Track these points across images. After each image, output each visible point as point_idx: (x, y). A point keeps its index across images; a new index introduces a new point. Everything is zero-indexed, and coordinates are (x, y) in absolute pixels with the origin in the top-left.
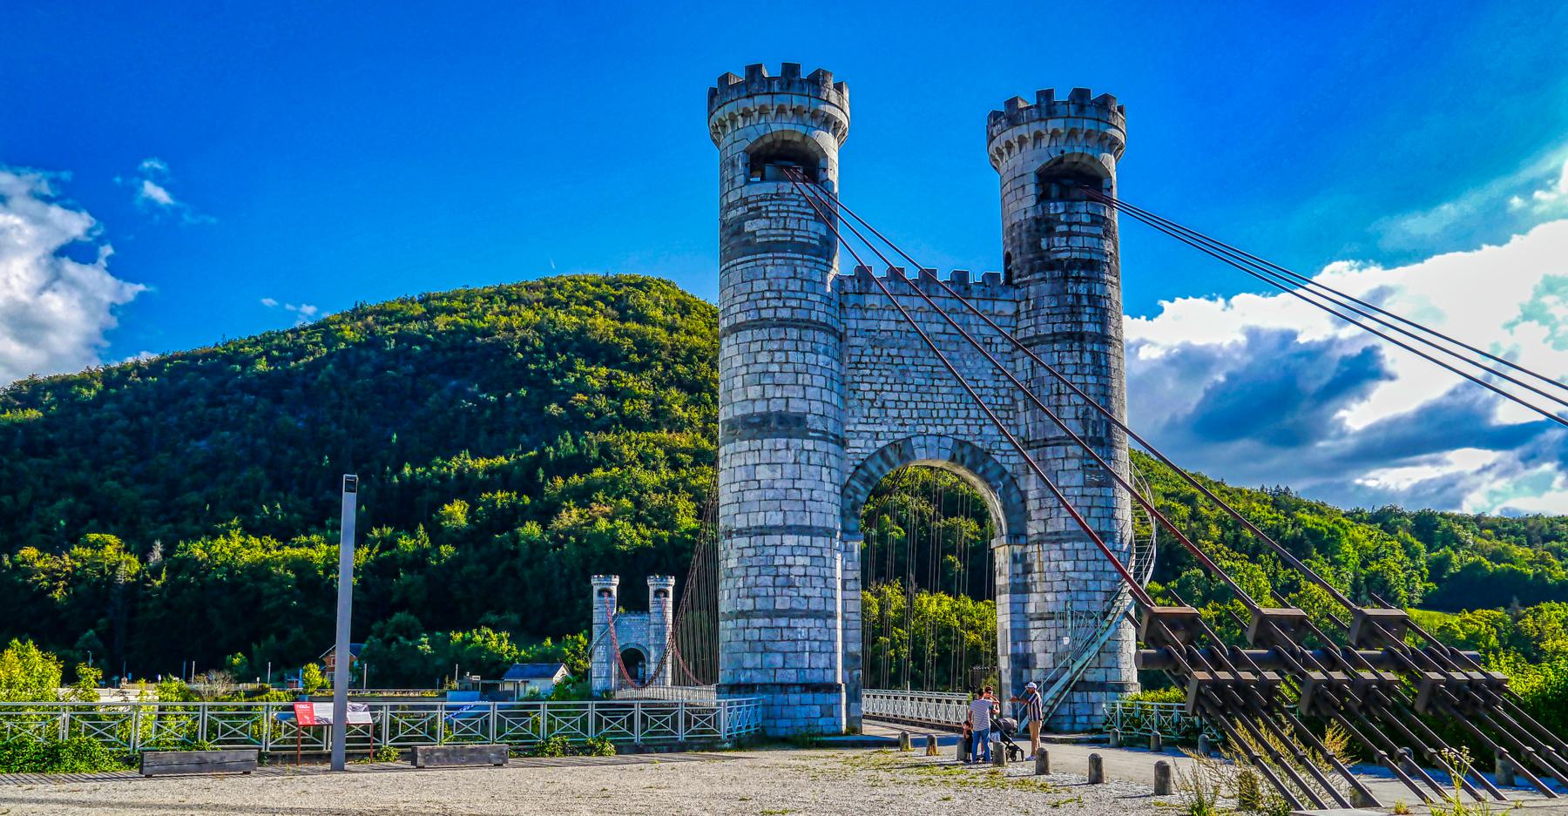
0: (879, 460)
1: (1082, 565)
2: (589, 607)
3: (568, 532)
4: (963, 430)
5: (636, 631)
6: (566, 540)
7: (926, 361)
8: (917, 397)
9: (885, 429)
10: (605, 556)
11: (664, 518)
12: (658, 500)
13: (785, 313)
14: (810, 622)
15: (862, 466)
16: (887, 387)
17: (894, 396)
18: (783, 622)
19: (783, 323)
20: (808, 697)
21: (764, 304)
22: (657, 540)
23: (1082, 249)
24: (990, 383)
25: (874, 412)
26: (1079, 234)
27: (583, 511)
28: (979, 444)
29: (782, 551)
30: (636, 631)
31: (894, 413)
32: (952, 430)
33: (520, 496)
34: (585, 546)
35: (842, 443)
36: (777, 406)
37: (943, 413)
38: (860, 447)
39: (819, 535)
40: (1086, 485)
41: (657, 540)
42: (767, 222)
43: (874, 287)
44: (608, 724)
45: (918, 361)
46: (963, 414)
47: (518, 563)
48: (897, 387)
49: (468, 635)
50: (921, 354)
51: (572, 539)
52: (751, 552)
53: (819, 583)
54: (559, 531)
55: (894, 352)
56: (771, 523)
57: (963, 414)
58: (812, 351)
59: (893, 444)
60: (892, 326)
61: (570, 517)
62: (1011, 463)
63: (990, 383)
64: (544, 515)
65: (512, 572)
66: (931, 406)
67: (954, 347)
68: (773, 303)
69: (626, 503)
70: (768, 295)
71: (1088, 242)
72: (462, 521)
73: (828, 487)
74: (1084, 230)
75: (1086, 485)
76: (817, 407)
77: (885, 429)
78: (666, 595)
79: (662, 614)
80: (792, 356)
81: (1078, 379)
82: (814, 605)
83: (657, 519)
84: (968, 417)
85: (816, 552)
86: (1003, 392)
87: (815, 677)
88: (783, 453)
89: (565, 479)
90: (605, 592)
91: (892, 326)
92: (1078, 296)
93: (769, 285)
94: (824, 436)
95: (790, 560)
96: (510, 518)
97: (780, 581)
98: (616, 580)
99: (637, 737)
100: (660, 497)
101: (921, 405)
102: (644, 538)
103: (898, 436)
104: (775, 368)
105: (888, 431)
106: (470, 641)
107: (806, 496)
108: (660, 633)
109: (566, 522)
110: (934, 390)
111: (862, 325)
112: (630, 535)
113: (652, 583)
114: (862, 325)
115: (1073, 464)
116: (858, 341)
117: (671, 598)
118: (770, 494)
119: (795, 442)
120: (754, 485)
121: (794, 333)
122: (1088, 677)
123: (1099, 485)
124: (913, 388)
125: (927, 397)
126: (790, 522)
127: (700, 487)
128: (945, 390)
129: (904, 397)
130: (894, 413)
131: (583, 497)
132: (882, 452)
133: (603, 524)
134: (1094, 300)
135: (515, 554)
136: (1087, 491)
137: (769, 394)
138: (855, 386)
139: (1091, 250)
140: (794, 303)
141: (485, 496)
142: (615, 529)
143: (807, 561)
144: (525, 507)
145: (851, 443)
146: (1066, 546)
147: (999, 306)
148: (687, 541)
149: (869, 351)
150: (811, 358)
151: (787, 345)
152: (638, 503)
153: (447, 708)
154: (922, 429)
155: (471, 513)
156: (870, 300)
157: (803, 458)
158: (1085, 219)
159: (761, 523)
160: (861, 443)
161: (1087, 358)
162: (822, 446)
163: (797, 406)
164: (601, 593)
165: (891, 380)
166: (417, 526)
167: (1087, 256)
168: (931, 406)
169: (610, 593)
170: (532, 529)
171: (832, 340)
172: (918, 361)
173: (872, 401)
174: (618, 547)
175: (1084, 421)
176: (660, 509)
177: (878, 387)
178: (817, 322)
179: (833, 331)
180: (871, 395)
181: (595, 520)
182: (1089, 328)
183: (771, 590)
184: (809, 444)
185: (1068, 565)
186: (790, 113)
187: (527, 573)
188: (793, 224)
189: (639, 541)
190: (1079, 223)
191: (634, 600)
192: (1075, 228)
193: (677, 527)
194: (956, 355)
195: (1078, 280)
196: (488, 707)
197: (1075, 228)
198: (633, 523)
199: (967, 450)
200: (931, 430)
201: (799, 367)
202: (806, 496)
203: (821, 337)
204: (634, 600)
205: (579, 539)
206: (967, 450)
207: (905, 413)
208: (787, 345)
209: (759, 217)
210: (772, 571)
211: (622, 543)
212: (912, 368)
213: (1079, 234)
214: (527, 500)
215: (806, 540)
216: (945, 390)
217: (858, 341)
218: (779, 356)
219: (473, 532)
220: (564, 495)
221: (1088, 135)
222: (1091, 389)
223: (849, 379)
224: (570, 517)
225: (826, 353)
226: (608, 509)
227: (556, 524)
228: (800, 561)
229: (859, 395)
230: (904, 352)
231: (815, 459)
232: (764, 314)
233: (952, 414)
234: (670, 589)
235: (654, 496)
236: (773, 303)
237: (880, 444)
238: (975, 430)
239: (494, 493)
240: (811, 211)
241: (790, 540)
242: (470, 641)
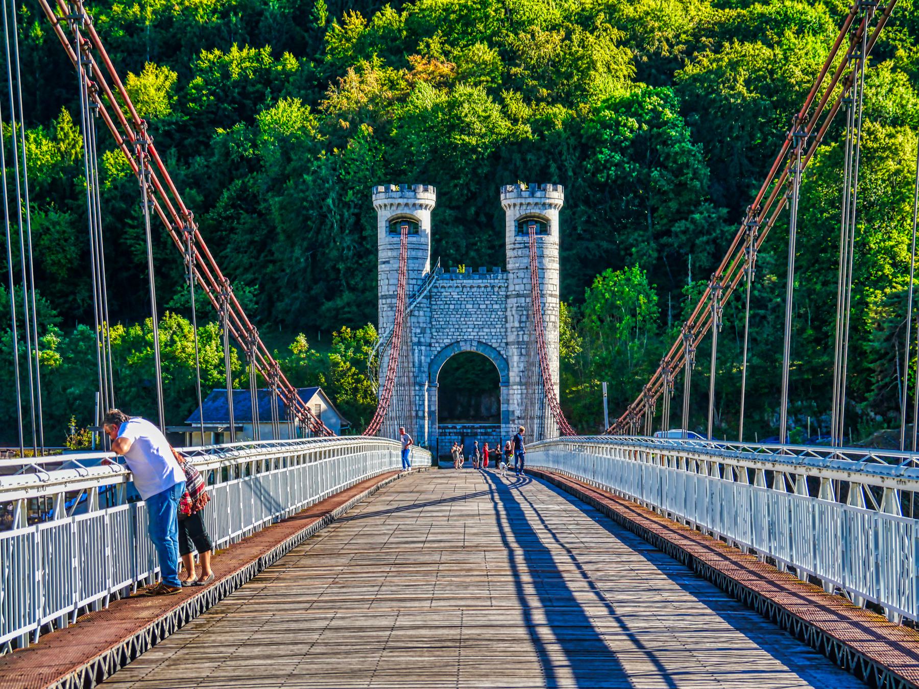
2: (367, 252)
3: (361, 115)
5: (472, 313)
6: (354, 130)
10: (422, 151)
11: (563, 78)
12: (551, 45)
22: (542, 125)
27: (391, 72)
30: (472, 313)
33: (277, 56)
34: (394, 143)
41: (542, 125)
47: (257, 182)
49: (136, 330)
51: (366, 129)
54: (343, 115)
61: (365, 83)
64: (313, 90)
65: (247, 201)
69: (483, 53)
72: (161, 106)
78: (544, 227)
79: (537, 274)
83: (550, 85)
89: (368, 16)
90: (404, 224)
96: (244, 100)
98: (428, 197)
100: (556, 38)
102: (515, 121)
106: (140, 343)
108: (532, 316)
109: (355, 94)
112: (486, 116)
113: (512, 202)
117: (554, 237)
127: (640, 21)
131: (397, 50)
133: (427, 96)
135: (254, 165)
141: (208, 57)
142: (453, 105)
144: (287, 74)
148: (605, 125)
152: (509, 56)
155: (179, 87)
164: (394, 226)
166: (56, 114)
169: (415, 226)
170: (288, 114)
174: (458, 138)
176: (555, 64)
181: (412, 85)
187: (275, 201)
189: (504, 126)
193: (585, 94)
198: (495, 94)
204: (471, 240)
205: (381, 132)
211: (467, 129)
214: (291, 62)
219: (182, 128)
220: (362, 48)
224: (365, 83)
226: (445, 69)
227: (336, 100)
234: (553, 216)
235: (542, 36)
239: (226, 50)
242: (140, 343)
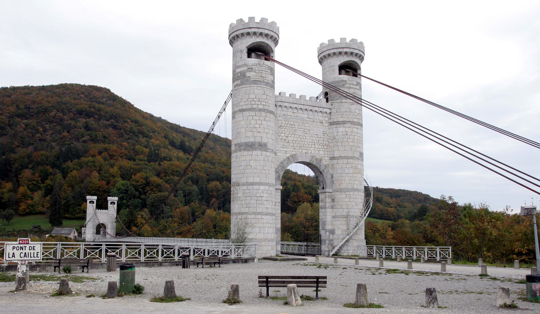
1: (352, 200)
4: (313, 152)
7: (302, 127)
8: (299, 139)
9: (288, 150)
13: (261, 107)
14: (267, 217)
15: (282, 163)
16: (290, 135)
18: (259, 216)
19: (260, 110)
20: (267, 243)
21: (254, 103)
24: (322, 136)
25: (286, 144)
26: (353, 88)
28: (318, 157)
29: (259, 191)
31: (292, 145)
32: (310, 151)
36: (258, 140)
37: (307, 146)
39: (270, 186)
42: (255, 74)
44: (149, 253)
45: (300, 127)
46: (313, 146)
48: (293, 136)
50: (301, 124)
52: (248, 191)
53: (270, 203)
55: (292, 123)
56: (256, 181)
58: (270, 121)
59: (292, 156)
63: (322, 136)
66: (303, 143)
67: (311, 123)
68: (257, 103)
70: (255, 99)
74: (354, 86)
77: (288, 150)
82: (270, 211)
84: (315, 148)
85: (270, 192)
86: (326, 139)
88: (260, 157)
91: (292, 114)
93: (256, 96)
95: (262, 195)
97: (258, 202)
99: (160, 259)
101: (301, 142)
103: (294, 153)
104: (257, 126)
110: (304, 137)
111: (282, 113)
114: (282, 113)
118: (256, 171)
119: (264, 153)
120: (249, 167)
121: (263, 114)
124: (298, 136)
125: (302, 140)
126: (262, 181)
128: (308, 138)
129: (295, 139)
130: (292, 145)
132: (288, 158)
137: (255, 135)
138: (279, 134)
140: (264, 103)
145: (278, 154)
146: (347, 193)
147: (325, 110)
149: (284, 122)
151: (262, 118)
153: (62, 245)
157: (266, 159)
159: (251, 181)
160: (281, 154)
163: (264, 140)
165: (291, 133)
168: (303, 143)
172: (300, 127)
173: (285, 140)
177: (286, 135)
178: (270, 111)
180: (285, 138)
183: (255, 205)
184: (268, 154)
185: (347, 200)
186: (264, 35)
188: (264, 75)
190: (354, 85)
191: (102, 205)
194: (311, 126)
196: (57, 244)
197: (352, 86)
202: (267, 172)
206: (314, 159)
207: (295, 145)
208: (262, 118)
209: (252, 71)
210: (256, 198)
212: (298, 129)
215: (267, 188)
216: (308, 138)
218: (259, 122)
223: (277, 132)
228: (265, 195)
229: (281, 137)
230: (295, 123)
232: (254, 106)
233: (310, 146)
236: (257, 103)
237: (288, 155)
238: (317, 152)
240: (269, 71)
241: (262, 187)
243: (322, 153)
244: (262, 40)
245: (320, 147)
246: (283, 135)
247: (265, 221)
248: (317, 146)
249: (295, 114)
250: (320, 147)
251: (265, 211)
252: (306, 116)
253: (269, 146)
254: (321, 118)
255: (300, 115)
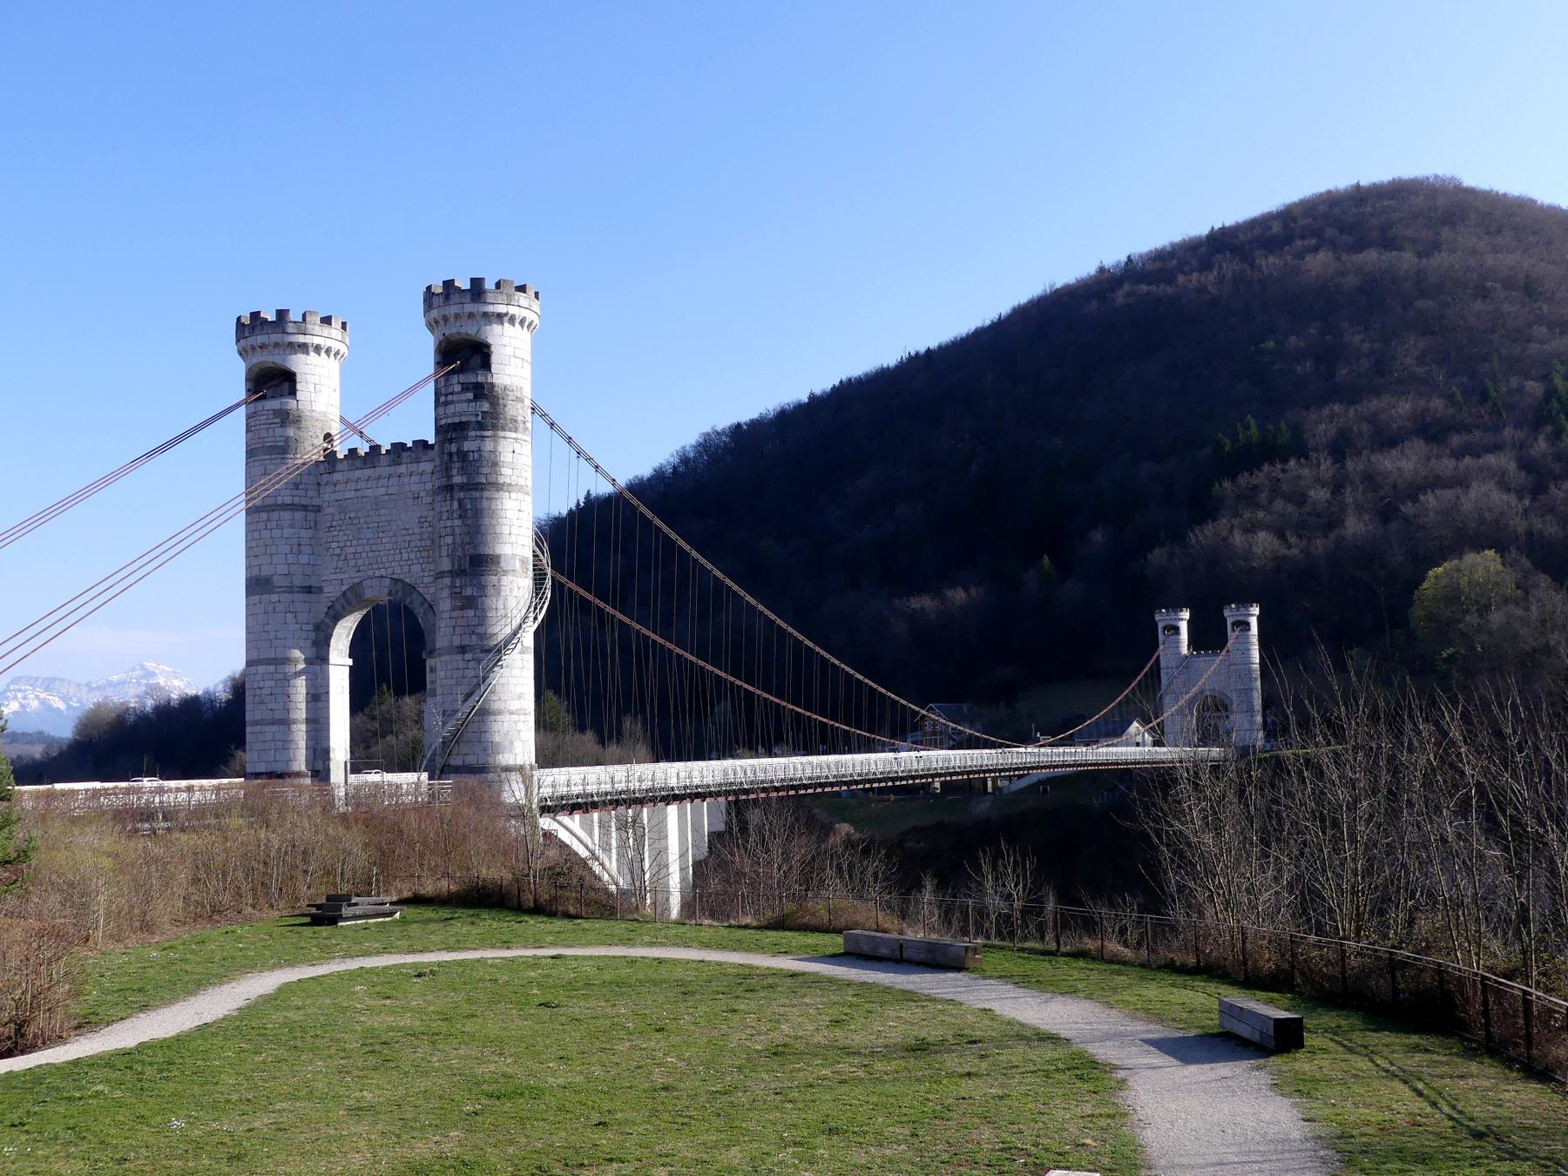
0: (342, 601)
4: (398, 570)
5: (1210, 672)
8: (367, 548)
14: (275, 728)
17: (352, 550)
23: (454, 415)
25: (340, 564)
26: (452, 402)
29: (258, 677)
35: (320, 590)
38: (332, 591)
40: (453, 609)
43: (339, 466)
46: (398, 557)
57: (398, 557)
60: (352, 494)
62: (429, 593)
71: (459, 407)
73: (293, 627)
74: (455, 398)
75: (453, 609)
76: (282, 569)
78: (1247, 625)
80: (266, 534)
81: (449, 523)
82: (278, 716)
86: (425, 536)
87: (279, 768)
92: (450, 454)
94: (290, 590)
105: (350, 578)
107: (272, 636)
113: (1230, 614)
115: (446, 593)
116: (330, 510)
119: (265, 597)
121: (264, 516)
122: (452, 762)
123: (462, 608)
129: (359, 549)
130: (352, 563)
134: (463, 456)
136: (455, 614)
139: (460, 414)
143: (272, 683)
150: (277, 533)
154: (371, 573)
156: (337, 477)
157: (270, 608)
158: (458, 388)
161: (456, 505)
162: (287, 597)
167: (457, 420)
171: (299, 515)
175: (451, 556)
179: (304, 508)
180: (338, 551)
182: (458, 479)
184: (274, 598)
188: (264, 434)
191: (1209, 636)
192: (450, 398)
195: (451, 441)
199: (400, 585)
200: (378, 574)
201: (268, 542)
203: (287, 515)
206: (400, 585)
207: (360, 562)
213: (452, 402)
217: (330, 510)
221: (457, 316)
222: (458, 531)
225: (292, 526)
228: (268, 684)
231: (279, 607)
237: (344, 588)
243: (416, 568)
244: (261, 359)
245: (412, 556)
246: (334, 545)
247: (270, 736)
248: (405, 556)
249: (359, 494)
250: (412, 556)
251: (268, 716)
252: (383, 491)
253: (277, 581)
254: (415, 488)
255: (369, 493)
